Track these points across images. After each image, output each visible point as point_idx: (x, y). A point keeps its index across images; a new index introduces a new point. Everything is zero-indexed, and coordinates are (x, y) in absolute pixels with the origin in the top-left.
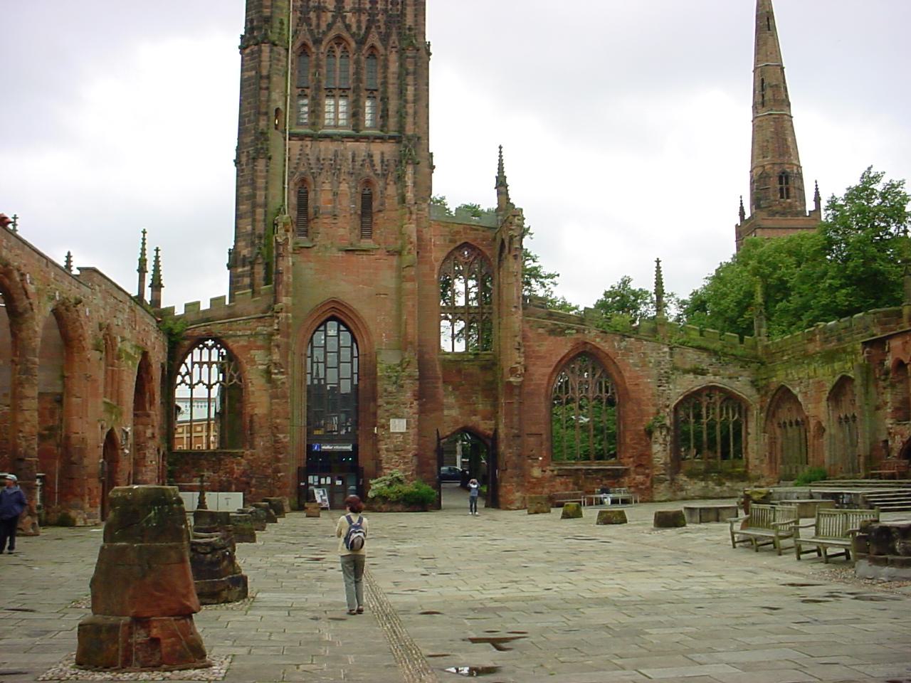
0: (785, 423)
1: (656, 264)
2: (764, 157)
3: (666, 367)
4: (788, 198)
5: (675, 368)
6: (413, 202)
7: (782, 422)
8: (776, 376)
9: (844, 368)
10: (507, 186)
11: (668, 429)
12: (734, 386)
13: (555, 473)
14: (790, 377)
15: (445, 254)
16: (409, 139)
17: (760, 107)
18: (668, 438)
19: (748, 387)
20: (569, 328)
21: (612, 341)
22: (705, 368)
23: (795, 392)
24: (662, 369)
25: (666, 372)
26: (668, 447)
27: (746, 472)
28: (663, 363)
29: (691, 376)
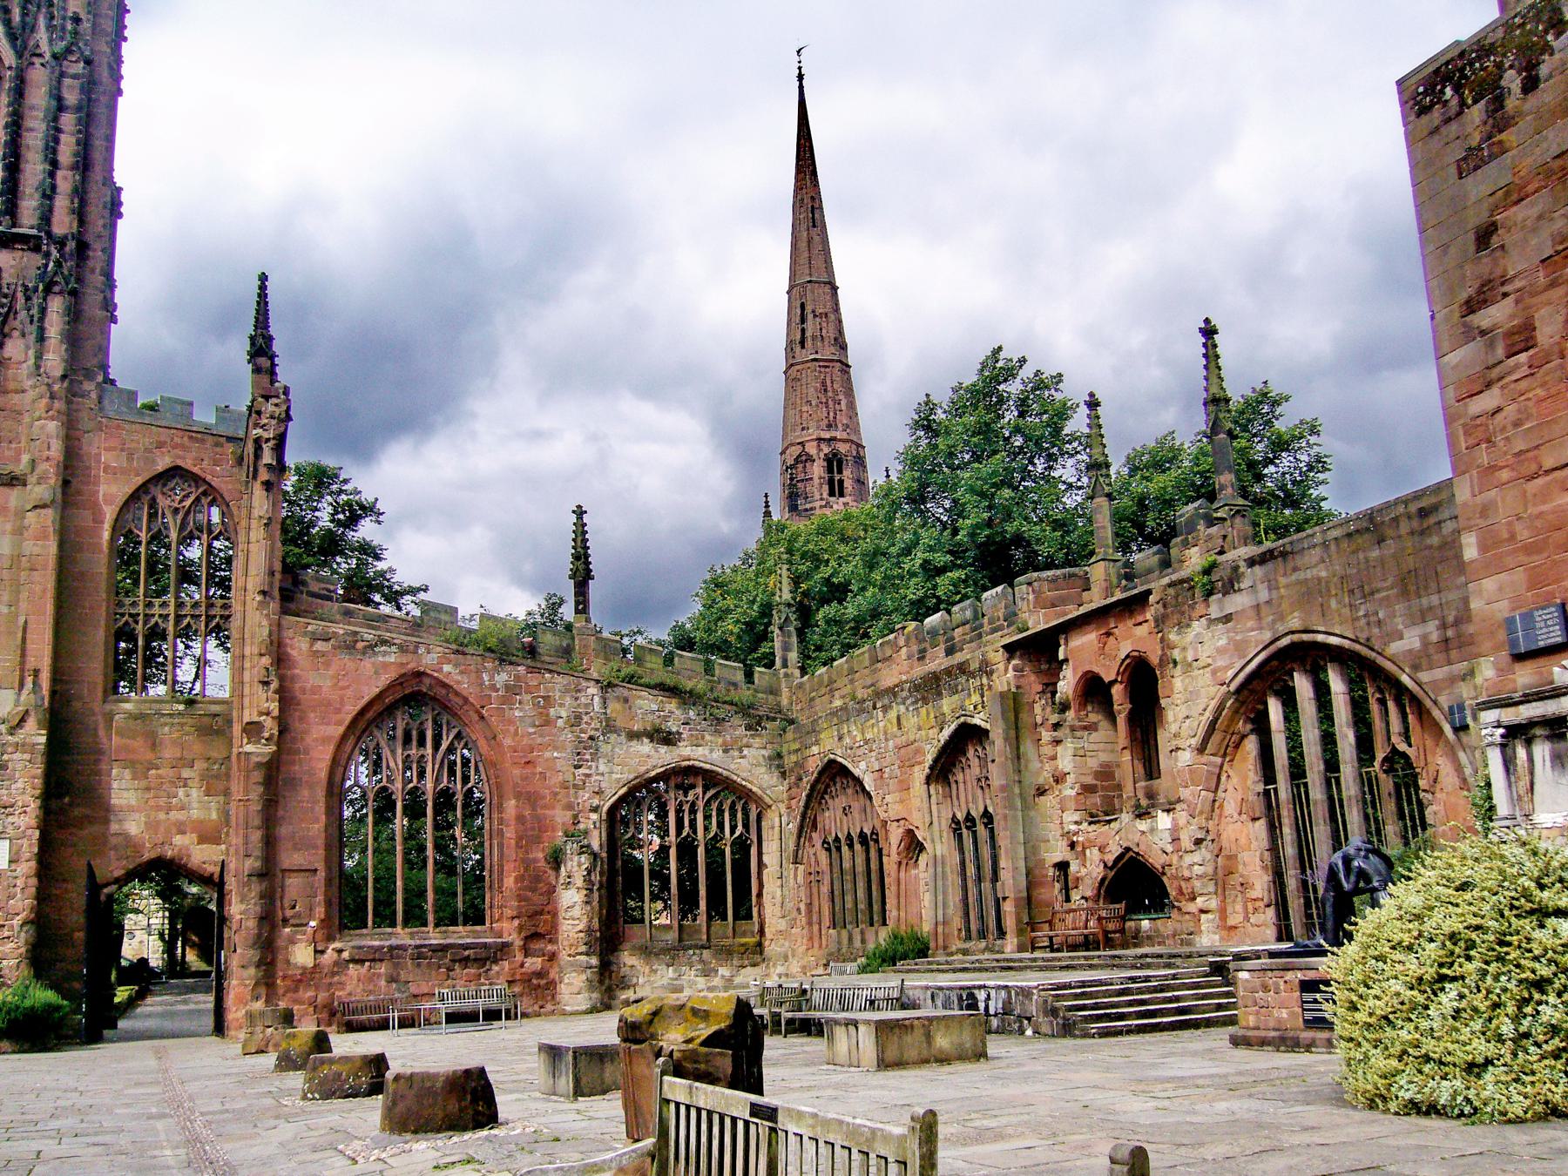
0: (837, 839)
1: (574, 518)
2: (803, 429)
3: (591, 726)
4: (842, 495)
5: (609, 727)
6: (58, 373)
7: (830, 840)
8: (817, 743)
9: (962, 708)
10: (272, 357)
11: (595, 855)
12: (732, 767)
13: (346, 955)
14: (847, 740)
15: (129, 490)
16: (61, 243)
17: (798, 349)
18: (596, 877)
19: (763, 770)
20: (384, 642)
21: (478, 671)
22: (674, 730)
23: (856, 772)
24: (582, 731)
25: (591, 738)
26: (596, 895)
27: (760, 944)
28: (586, 718)
29: (645, 747)
